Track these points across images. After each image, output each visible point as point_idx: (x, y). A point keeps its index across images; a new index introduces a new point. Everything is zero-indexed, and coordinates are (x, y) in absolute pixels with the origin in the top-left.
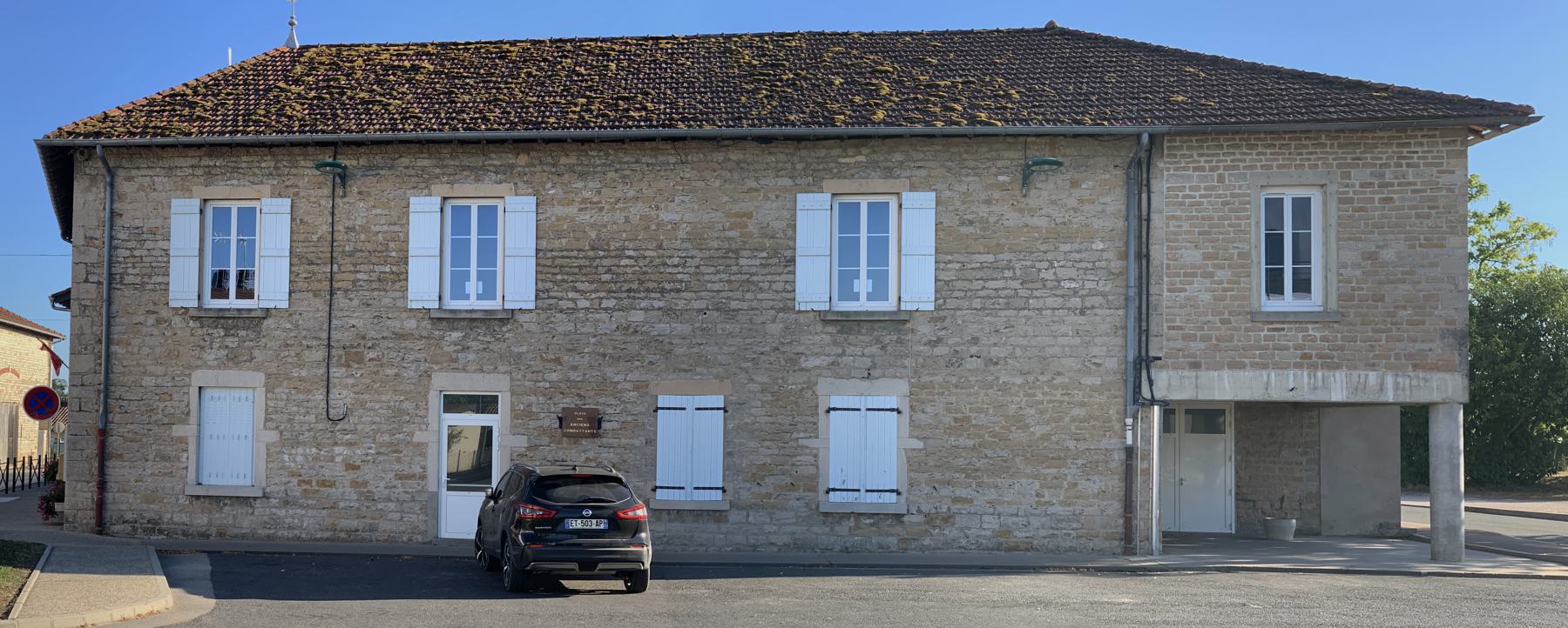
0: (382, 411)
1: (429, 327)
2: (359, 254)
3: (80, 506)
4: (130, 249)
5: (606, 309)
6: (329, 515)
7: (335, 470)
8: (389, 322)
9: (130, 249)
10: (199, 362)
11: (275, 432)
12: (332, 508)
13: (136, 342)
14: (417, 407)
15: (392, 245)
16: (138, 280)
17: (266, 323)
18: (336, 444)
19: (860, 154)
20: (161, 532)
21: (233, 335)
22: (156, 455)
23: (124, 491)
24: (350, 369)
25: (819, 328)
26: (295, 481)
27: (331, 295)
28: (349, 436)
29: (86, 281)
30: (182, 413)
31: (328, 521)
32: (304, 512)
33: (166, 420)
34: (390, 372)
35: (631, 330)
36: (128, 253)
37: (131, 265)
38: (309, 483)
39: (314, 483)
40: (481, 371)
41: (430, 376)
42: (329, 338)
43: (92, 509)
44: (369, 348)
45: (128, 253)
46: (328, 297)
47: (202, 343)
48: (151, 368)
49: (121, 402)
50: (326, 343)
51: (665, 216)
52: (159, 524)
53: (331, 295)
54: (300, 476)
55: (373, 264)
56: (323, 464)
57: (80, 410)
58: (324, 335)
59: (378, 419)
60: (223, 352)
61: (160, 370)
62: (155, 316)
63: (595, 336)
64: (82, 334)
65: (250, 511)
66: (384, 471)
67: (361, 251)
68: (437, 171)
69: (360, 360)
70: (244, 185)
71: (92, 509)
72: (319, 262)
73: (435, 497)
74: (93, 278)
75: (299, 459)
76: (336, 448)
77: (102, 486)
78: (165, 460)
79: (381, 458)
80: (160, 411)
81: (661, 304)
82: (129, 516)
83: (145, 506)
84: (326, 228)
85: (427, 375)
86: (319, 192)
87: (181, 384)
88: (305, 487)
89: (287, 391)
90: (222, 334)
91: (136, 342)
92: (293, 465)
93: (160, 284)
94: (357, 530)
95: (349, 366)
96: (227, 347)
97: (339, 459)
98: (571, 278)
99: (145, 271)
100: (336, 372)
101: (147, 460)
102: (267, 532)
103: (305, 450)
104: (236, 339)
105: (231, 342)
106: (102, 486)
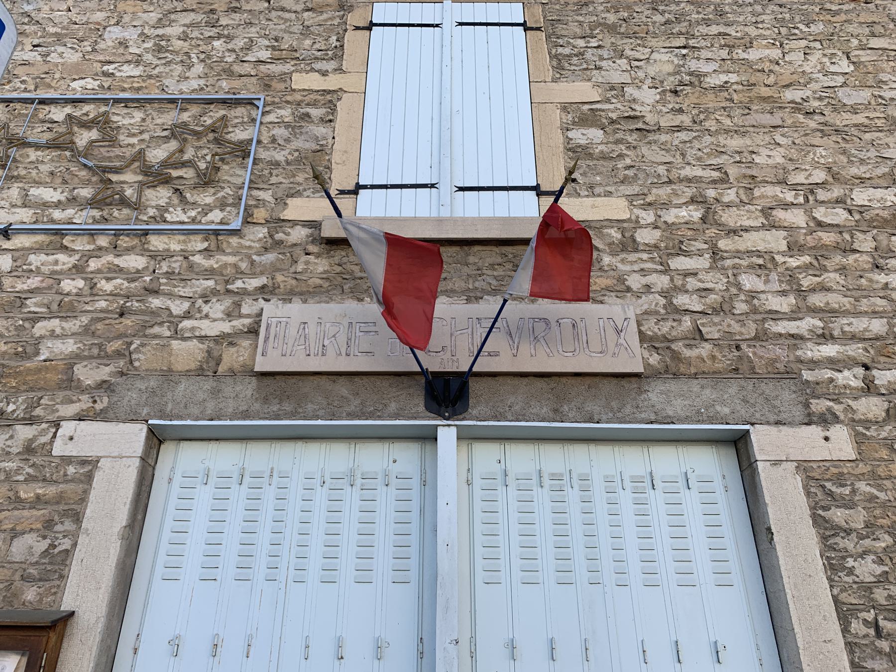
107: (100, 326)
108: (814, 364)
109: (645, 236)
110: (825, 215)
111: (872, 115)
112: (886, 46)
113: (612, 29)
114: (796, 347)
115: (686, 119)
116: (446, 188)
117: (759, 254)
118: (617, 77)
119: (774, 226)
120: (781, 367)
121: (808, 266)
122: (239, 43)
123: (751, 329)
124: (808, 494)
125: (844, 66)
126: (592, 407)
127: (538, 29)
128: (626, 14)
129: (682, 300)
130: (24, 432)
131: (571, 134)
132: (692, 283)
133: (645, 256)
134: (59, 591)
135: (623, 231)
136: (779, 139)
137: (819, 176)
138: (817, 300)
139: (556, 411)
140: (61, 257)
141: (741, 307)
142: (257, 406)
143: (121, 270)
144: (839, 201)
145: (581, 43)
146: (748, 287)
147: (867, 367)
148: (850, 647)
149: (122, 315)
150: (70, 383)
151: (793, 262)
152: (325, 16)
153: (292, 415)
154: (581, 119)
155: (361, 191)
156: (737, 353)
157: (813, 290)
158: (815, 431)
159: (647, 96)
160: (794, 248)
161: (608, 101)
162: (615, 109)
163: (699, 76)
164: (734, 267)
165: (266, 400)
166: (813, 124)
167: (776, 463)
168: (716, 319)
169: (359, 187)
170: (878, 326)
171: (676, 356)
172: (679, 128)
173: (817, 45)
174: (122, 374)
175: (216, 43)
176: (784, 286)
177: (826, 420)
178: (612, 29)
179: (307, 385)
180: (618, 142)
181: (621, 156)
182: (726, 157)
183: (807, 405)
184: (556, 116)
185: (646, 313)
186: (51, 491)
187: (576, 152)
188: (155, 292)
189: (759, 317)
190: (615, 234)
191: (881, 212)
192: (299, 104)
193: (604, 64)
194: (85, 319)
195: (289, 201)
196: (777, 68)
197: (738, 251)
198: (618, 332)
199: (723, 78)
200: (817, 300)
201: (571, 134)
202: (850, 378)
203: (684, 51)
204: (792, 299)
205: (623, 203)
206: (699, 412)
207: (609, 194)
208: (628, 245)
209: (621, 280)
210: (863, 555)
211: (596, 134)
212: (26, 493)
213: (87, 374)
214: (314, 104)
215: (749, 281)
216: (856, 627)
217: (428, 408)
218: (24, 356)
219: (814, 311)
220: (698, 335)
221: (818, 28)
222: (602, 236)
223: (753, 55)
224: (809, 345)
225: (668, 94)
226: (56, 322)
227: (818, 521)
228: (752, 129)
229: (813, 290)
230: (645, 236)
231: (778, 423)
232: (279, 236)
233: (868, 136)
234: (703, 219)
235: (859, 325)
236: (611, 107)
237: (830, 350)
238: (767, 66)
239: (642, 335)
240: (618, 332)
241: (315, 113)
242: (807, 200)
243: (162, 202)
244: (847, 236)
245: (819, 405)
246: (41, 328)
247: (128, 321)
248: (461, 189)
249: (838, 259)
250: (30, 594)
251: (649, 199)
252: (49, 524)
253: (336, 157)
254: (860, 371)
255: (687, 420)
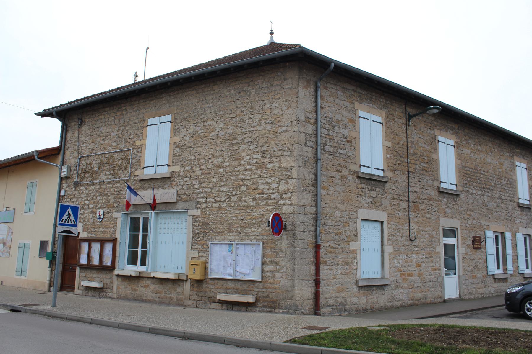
0: (426, 236)
1: (438, 195)
2: (416, 156)
3: (305, 298)
4: (328, 130)
5: (479, 194)
6: (412, 292)
7: (412, 268)
8: (426, 191)
9: (328, 130)
10: (360, 205)
11: (392, 247)
12: (413, 288)
13: (332, 188)
14: (436, 234)
15: (425, 153)
16: (331, 149)
17: (387, 185)
18: (413, 253)
19: (518, 149)
20: (346, 310)
21: (374, 190)
22: (343, 262)
23: (328, 286)
24: (415, 214)
25: (517, 208)
26: (399, 273)
27: (409, 174)
28: (416, 249)
29: (306, 145)
30: (354, 235)
31: (411, 295)
32: (403, 291)
33: (346, 239)
34: (428, 216)
35: (485, 204)
36: (326, 132)
37: (328, 140)
38: (404, 275)
39: (406, 275)
40: (452, 217)
41: (439, 219)
42: (408, 197)
43: (311, 299)
44: (421, 203)
45: (326, 132)
46: (407, 175)
47: (361, 193)
48: (338, 205)
49: (325, 227)
50: (407, 199)
51: (488, 160)
52: (345, 305)
53: (409, 174)
54: (401, 271)
55: (421, 161)
56: (409, 264)
57: (304, 231)
58: (407, 195)
59: (425, 240)
60: (370, 200)
61: (343, 207)
62: (340, 173)
63: (478, 205)
64: (304, 179)
65: (383, 293)
66: (428, 267)
67: (416, 154)
68: (436, 123)
69: (418, 210)
70: (375, 108)
71: (311, 299)
72: (403, 156)
73: (443, 277)
74: (309, 144)
75: (401, 261)
76: (414, 255)
77: (317, 283)
78: (347, 264)
79: (427, 260)
80: (343, 233)
81: (490, 195)
82: (331, 302)
83: (338, 295)
84: (405, 140)
85: (438, 218)
86: (401, 121)
87: (353, 216)
88: (403, 277)
89: (395, 224)
90: (370, 189)
91: (332, 188)
92: (398, 265)
93: (342, 154)
94: (421, 299)
95: (415, 212)
96: (371, 196)
97: (414, 261)
98: (471, 180)
99: (335, 145)
100: (412, 215)
101: (338, 265)
102: (390, 304)
103: (402, 257)
104: (375, 193)
105: (373, 193)
106: (317, 283)
107: (116, 197)
108: (199, 198)
109: (182, 174)
110: (209, 166)
111: (223, 139)
112: (232, 117)
113: (185, 119)
114: (197, 195)
115: (192, 144)
116: (155, 166)
117: (196, 176)
118: (183, 134)
119: (201, 169)
120: (194, 199)
121: (203, 178)
122: (129, 134)
123: (192, 193)
124: (193, 221)
125: (222, 125)
126: (170, 207)
127: (173, 122)
128: (188, 114)
129: (184, 187)
130: (110, 214)
131: (175, 151)
132: (186, 183)
133: (180, 178)
134: (115, 235)
135: (179, 173)
136: (206, 148)
137: (210, 156)
138: (202, 185)
139: (166, 208)
140: (110, 185)
141: (192, 188)
142: (133, 209)
143: (117, 187)
144: (212, 162)
145: (179, 125)
146: (193, 183)
147: (206, 198)
148: (192, 242)
149: (118, 195)
150: (114, 207)
151: (201, 178)
152: (141, 124)
153: (136, 211)
154: (177, 147)
155: (145, 168)
156: (189, 197)
157: (203, 183)
158: (196, 210)
159: (187, 138)
160: (202, 174)
161: (181, 141)
162: (183, 142)
163: (197, 131)
164: (193, 179)
165: (134, 208)
166: (213, 143)
167: (190, 216)
168: (188, 190)
169: (144, 167)
170: (209, 190)
171: (182, 198)
172: (191, 147)
173: (219, 118)
174: (118, 205)
175: (126, 135)
176: (199, 183)
177: (197, 208)
178: (185, 119)
179: (138, 206)
180: (182, 151)
181: (181, 155)
182: (197, 153)
183: (196, 206)
184: (173, 146)
185: (179, 190)
186: (114, 222)
187: (175, 155)
188: (121, 191)
189: (194, 190)
190: (177, 174)
191: (217, 165)
192: (137, 148)
193: (182, 130)
194: (114, 196)
195: (136, 171)
196: (211, 127)
197: (194, 176)
198: (174, 194)
199: (201, 131)
200: (202, 185)
201: (175, 151)
202: (203, 200)
203: (196, 124)
204: (199, 186)
205: (179, 167)
206: (182, 208)
207: (178, 165)
208: (179, 176)
209: (177, 183)
210: (197, 230)
211: (178, 150)
212: (112, 223)
213: (116, 205)
214: (139, 148)
215: (194, 182)
216: (194, 239)
217: (151, 209)
218: (109, 202)
219: (202, 187)
220: (185, 194)
221: (221, 113)
222: (176, 174)
223: (207, 124)
224: (199, 194)
225: (191, 137)
226: (111, 197)
227: (193, 224)
228: (202, 145)
229: (203, 183)
230: (182, 174)
231: (192, 209)
232: (135, 179)
233: (221, 145)
234: (191, 169)
235: (207, 190)
236: (181, 142)
237: (202, 195)
238: (208, 127)
239: (178, 194)
240: (174, 194)
241: (139, 150)
242: (207, 163)
243: (121, 173)
244: (210, 171)
245: (198, 206)
246: (110, 197)
247: (119, 196)
248: (158, 166)
249: (208, 176)
250: (113, 236)
251: (184, 165)
252: (114, 227)
253: (141, 161)
254: (205, 199)
255: (181, 209)
